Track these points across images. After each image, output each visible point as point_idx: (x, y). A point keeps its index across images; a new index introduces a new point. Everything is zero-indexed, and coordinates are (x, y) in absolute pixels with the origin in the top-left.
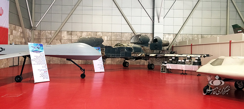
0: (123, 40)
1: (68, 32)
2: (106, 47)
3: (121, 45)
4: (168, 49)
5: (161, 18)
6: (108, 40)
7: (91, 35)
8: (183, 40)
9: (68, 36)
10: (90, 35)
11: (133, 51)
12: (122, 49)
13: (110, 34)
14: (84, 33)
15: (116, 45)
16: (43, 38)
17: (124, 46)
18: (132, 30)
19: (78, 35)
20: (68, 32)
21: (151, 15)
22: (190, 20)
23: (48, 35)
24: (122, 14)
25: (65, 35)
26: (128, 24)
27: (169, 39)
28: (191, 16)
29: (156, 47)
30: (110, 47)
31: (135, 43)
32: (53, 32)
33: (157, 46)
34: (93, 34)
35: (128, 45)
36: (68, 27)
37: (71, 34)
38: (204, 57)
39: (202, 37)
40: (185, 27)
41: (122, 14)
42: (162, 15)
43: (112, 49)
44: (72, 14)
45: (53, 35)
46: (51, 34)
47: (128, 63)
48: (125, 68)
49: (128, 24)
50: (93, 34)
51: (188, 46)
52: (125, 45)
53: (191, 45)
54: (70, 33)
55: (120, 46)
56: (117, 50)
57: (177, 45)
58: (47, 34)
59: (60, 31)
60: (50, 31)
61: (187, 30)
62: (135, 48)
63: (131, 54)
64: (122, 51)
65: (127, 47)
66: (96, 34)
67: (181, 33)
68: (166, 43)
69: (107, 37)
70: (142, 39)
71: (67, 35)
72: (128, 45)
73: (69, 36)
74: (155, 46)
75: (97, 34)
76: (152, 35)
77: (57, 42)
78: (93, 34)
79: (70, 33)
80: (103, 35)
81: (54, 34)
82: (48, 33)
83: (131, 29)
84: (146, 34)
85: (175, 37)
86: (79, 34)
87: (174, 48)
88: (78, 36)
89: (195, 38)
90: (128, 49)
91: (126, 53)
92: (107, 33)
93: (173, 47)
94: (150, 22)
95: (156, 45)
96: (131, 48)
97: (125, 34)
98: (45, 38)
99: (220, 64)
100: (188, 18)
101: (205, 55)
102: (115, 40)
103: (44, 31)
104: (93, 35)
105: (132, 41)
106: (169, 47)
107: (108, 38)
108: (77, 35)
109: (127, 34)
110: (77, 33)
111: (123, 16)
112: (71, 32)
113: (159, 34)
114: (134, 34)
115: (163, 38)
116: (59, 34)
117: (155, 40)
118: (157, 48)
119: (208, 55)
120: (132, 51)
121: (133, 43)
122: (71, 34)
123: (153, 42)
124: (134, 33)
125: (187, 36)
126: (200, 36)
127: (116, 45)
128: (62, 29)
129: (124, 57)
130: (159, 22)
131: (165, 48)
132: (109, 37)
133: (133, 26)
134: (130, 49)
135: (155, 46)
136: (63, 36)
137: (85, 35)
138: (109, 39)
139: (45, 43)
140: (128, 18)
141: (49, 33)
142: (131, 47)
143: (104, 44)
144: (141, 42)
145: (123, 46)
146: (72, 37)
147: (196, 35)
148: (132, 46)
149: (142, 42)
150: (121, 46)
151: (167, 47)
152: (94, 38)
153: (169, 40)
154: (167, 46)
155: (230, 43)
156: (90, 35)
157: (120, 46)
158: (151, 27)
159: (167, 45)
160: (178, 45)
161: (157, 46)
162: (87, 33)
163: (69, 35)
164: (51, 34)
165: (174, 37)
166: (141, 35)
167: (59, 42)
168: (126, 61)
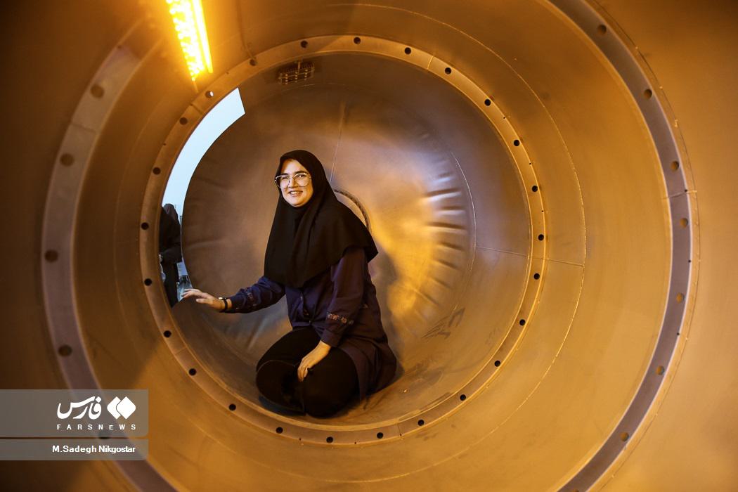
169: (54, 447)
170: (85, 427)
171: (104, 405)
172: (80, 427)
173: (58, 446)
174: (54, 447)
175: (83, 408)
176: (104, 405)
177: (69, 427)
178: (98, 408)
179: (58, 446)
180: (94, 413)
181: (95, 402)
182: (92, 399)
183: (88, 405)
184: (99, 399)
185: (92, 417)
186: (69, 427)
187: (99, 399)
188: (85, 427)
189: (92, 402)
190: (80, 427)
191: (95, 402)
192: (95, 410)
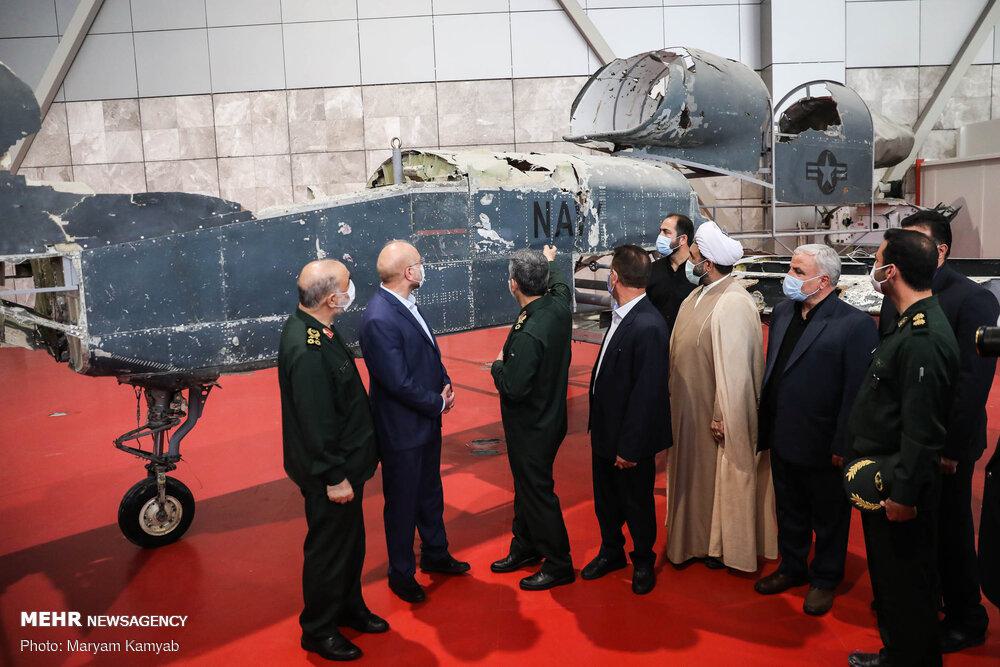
2: (97, 218)
3: (430, 172)
7: (280, 117)
10: (273, 115)
11: (593, 241)
12: (431, 222)
15: (381, 173)
17: (453, 188)
19: (187, 124)
20: (111, 103)
29: (827, 170)
31: (620, 144)
33: (833, 162)
34: (293, 103)
35: (524, 166)
37: (136, 122)
43: (233, 235)
62: (613, 198)
65: (505, 198)
66: (320, 110)
69: (405, 123)
70: (696, 93)
71: (108, 130)
72: (524, 166)
73: (126, 139)
74: (821, 162)
75: (328, 106)
78: (293, 103)
80: (372, 110)
85: (937, 92)
88: (185, 132)
90: (528, 215)
95: (827, 157)
97: (544, 87)
104: (293, 114)
105: (586, 123)
107: (415, 133)
108: (175, 125)
110: (179, 111)
112: (132, 105)
117: (816, 113)
118: (835, 179)
120: (584, 232)
122: (136, 122)
132: (418, 120)
135: (821, 162)
136: (83, 143)
137: (236, 120)
138: (421, 133)
142: (572, 186)
144: (684, 121)
146: (147, 139)
148: (573, 171)
149: (696, 121)
150: (429, 188)
161: (833, 162)
162: (251, 106)
163: (122, 125)
165: (927, 94)
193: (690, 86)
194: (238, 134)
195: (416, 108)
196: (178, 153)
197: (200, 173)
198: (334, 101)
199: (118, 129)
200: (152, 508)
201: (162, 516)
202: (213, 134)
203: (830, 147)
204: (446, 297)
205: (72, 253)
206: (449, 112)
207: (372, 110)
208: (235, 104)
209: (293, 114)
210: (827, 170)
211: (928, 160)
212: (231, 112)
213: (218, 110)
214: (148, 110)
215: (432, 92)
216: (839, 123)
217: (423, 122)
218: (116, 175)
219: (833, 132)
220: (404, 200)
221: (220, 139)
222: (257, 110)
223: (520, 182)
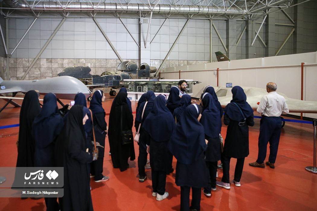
0: (108, 66)
1: (47, 59)
2: (94, 76)
3: (109, 74)
4: (155, 76)
5: (148, 44)
6: (92, 67)
8: (170, 66)
9: (47, 63)
10: (72, 62)
13: (94, 61)
14: (66, 61)
16: (19, 66)
17: (112, 75)
18: (118, 56)
20: (47, 59)
21: (137, 41)
22: (176, 45)
23: (25, 63)
24: (106, 39)
25: (44, 63)
26: (113, 50)
27: (154, 64)
28: (177, 42)
29: (144, 73)
30: (97, 76)
31: (122, 71)
32: (30, 59)
33: (145, 73)
34: (75, 61)
35: (116, 73)
36: (48, 54)
37: (51, 62)
38: (194, 84)
39: (188, 64)
40: (171, 53)
41: (106, 39)
42: (149, 39)
44: (51, 40)
45: (31, 63)
46: (28, 62)
47: (115, 91)
48: (112, 97)
49: (113, 50)
50: (76, 61)
51: (176, 73)
52: (113, 73)
53: (180, 72)
54: (50, 60)
55: (107, 74)
56: (105, 79)
57: (164, 71)
58: (24, 62)
59: (39, 59)
60: (28, 59)
61: (173, 56)
63: (119, 82)
64: (110, 80)
65: (115, 76)
66: (79, 62)
67: (168, 58)
68: (153, 69)
69: (91, 64)
71: (47, 63)
72: (116, 73)
73: (50, 64)
75: (80, 61)
76: (139, 61)
77: (36, 71)
79: (50, 60)
80: (86, 62)
81: (32, 62)
82: (25, 61)
83: (116, 55)
84: (132, 60)
86: (60, 62)
87: (162, 74)
88: (59, 64)
89: (181, 64)
91: (114, 82)
92: (91, 59)
93: (160, 73)
94: (137, 48)
96: (119, 77)
97: (110, 60)
98: (22, 66)
99: (225, 95)
100: (174, 44)
101: (195, 82)
102: (100, 67)
103: (20, 59)
104: (75, 62)
105: (119, 68)
106: (156, 73)
108: (57, 63)
109: (112, 61)
111: (107, 42)
112: (51, 59)
113: (145, 60)
114: (119, 60)
115: (150, 64)
116: (38, 62)
117: (143, 67)
119: (197, 82)
120: (121, 79)
121: (121, 70)
122: (51, 62)
123: (141, 69)
124: (119, 59)
125: (173, 62)
126: (186, 62)
127: (103, 74)
128: (42, 57)
129: (112, 86)
130: (145, 48)
131: (152, 75)
132: (93, 64)
133: (118, 52)
134: (118, 78)
136: (43, 64)
138: (93, 66)
139: (22, 71)
140: (113, 44)
141: (27, 61)
142: (119, 75)
143: (92, 73)
144: (129, 69)
145: (111, 74)
146: (53, 64)
147: (182, 61)
148: (120, 73)
149: (130, 69)
150: (109, 75)
151: (155, 74)
152: (81, 67)
153: (156, 65)
154: (154, 72)
155: (218, 70)
156: (72, 62)
157: (108, 75)
158: (137, 52)
159: (154, 71)
160: (165, 71)
161: (145, 73)
162: (69, 61)
164: (28, 62)
165: (161, 63)
166: (128, 62)
167: (38, 70)
168: (113, 89)
169: (23, 191)
170: (37, 183)
171: (45, 174)
172: (34, 183)
173: (25, 191)
174: (23, 191)
175: (35, 175)
176: (45, 174)
177: (30, 183)
178: (42, 175)
179: (25, 191)
180: (40, 177)
181: (41, 172)
182: (40, 171)
183: (38, 174)
184: (42, 171)
185: (40, 179)
186: (30, 183)
187: (42, 171)
188: (37, 183)
189: (39, 172)
190: (34, 183)
191: (41, 172)
192: (41, 176)
193: (130, 66)
194: (67, 64)
195: (93, 62)
196: (57, 66)
197: (60, 70)
198: (81, 61)
199: (48, 63)
200: (90, 98)
201: (90, 99)
202: (63, 64)
203: (145, 71)
204: (111, 83)
205: (92, 78)
206: (97, 63)
207: (86, 62)
208: (67, 60)
209: (75, 62)
210: (144, 73)
211: (161, 72)
212: (66, 61)
213: (64, 61)
214: (53, 61)
215: (95, 60)
216: (145, 68)
217: (94, 64)
218: (47, 69)
219: (145, 69)
220: (108, 76)
221: (64, 65)
222: (70, 61)
223: (116, 75)
